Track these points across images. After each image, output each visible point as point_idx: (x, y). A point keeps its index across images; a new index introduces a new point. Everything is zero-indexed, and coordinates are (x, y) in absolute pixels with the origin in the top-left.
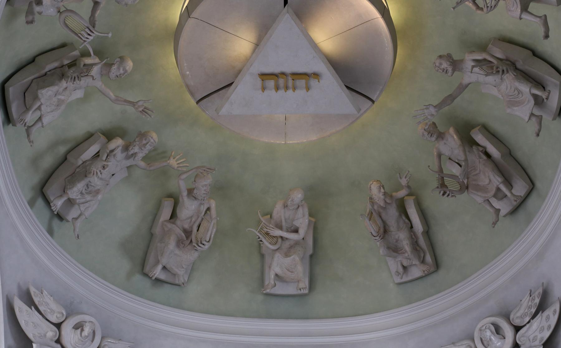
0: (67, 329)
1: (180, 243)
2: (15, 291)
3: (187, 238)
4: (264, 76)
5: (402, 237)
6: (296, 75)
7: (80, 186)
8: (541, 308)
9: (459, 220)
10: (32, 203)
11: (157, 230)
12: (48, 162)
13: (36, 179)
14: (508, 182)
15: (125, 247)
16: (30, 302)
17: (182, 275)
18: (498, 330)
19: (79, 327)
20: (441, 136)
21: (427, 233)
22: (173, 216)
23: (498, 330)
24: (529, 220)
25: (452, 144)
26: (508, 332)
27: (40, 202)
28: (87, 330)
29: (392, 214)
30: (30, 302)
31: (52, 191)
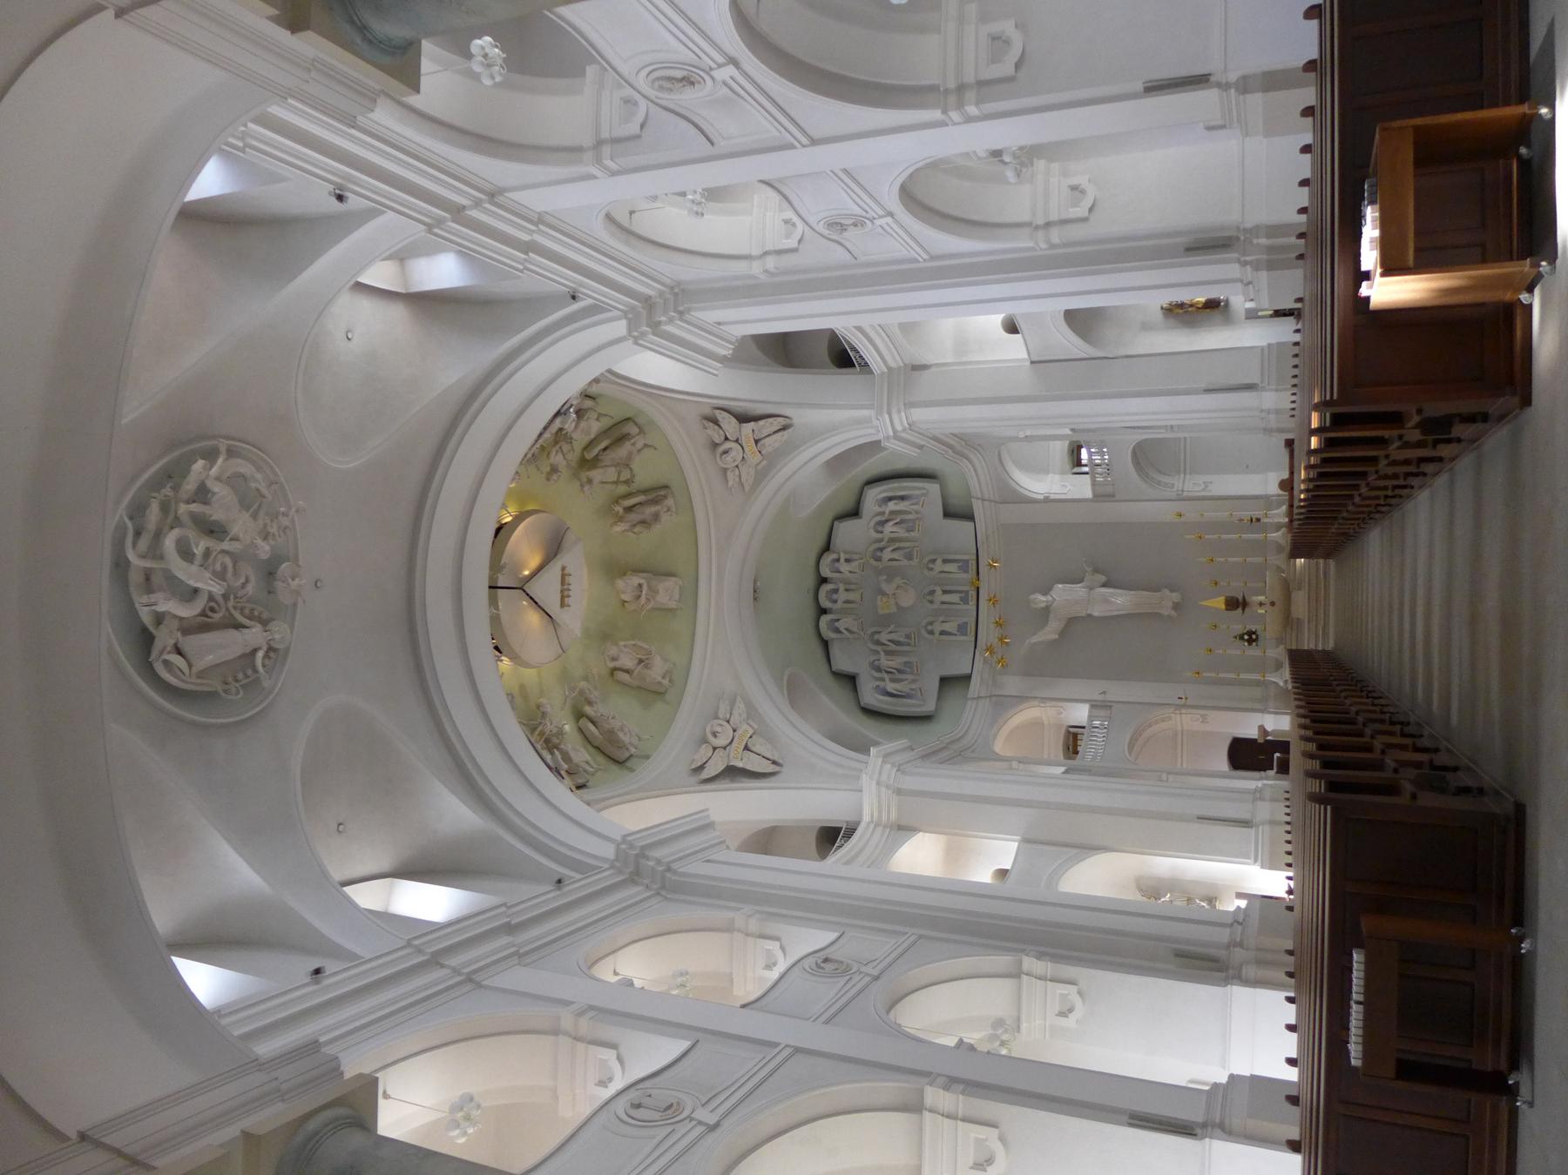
2: (694, 779)
7: (621, 735)
8: (716, 422)
10: (632, 770)
12: (601, 759)
13: (614, 767)
14: (623, 438)
16: (702, 767)
18: (726, 452)
20: (590, 481)
23: (726, 452)
25: (596, 475)
26: (727, 445)
27: (628, 764)
28: (719, 729)
30: (702, 767)
31: (623, 755)
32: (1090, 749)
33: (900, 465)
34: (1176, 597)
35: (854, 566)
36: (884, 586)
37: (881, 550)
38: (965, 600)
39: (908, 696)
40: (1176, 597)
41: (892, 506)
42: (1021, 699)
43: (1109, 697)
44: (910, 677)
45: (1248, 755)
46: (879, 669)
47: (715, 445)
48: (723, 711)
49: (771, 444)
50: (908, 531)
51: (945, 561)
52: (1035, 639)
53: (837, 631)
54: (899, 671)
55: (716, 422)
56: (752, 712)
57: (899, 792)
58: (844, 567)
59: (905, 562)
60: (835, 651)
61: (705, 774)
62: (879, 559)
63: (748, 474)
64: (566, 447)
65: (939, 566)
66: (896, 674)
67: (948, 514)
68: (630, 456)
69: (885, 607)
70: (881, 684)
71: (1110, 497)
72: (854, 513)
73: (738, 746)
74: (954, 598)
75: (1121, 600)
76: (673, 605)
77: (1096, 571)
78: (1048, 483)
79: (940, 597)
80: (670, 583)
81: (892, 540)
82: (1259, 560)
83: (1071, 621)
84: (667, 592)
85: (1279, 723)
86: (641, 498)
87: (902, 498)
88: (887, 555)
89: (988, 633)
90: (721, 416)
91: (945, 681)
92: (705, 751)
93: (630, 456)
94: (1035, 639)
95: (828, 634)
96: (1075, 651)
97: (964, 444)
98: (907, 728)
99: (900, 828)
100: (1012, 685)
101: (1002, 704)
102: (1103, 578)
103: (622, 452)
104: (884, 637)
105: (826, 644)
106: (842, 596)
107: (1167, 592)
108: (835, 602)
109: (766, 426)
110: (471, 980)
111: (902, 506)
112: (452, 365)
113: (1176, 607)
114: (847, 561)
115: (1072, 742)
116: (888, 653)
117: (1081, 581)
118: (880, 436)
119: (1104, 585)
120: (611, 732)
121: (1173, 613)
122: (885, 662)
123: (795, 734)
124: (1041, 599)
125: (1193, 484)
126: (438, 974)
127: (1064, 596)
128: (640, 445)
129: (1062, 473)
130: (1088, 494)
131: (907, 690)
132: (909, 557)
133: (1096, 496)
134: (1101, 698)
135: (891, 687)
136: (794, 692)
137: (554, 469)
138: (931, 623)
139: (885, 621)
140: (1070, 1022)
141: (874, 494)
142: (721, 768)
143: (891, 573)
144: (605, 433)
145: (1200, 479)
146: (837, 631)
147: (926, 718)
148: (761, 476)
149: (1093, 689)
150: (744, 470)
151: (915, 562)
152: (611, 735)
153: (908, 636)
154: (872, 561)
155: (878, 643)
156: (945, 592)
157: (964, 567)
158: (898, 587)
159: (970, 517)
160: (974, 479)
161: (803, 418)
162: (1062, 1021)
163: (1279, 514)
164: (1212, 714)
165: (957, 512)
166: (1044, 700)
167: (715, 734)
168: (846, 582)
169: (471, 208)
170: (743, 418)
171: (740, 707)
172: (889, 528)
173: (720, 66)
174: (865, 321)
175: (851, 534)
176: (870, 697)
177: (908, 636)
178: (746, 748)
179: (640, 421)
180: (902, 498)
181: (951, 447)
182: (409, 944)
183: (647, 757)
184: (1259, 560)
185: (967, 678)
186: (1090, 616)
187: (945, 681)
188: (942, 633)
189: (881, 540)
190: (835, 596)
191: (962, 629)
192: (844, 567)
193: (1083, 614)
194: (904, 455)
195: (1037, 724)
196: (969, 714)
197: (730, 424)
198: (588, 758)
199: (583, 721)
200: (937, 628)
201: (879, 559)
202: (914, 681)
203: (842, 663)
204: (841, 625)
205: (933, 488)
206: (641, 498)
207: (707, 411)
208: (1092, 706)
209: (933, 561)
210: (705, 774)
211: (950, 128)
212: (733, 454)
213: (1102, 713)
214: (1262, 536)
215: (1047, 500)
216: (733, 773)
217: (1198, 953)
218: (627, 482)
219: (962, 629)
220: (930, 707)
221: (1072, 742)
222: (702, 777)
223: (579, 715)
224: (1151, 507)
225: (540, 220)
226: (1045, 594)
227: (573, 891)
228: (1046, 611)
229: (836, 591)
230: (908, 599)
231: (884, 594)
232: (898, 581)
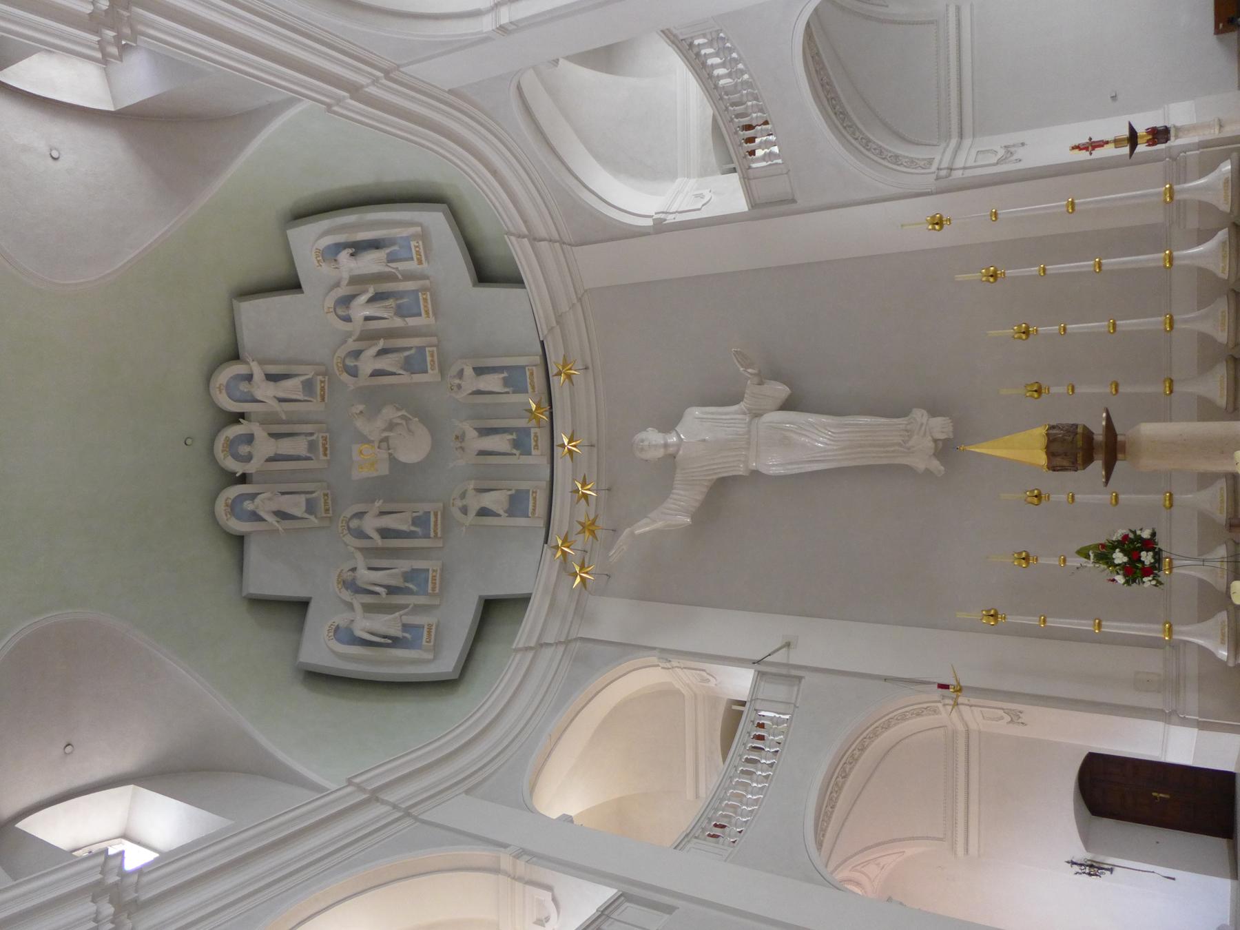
33: (359, 173)
34: (940, 427)
35: (291, 388)
36: (360, 423)
37: (357, 354)
38: (521, 443)
39: (396, 642)
40: (940, 427)
41: (348, 265)
42: (627, 649)
43: (798, 657)
44: (421, 600)
46: (354, 587)
50: (401, 312)
51: (480, 371)
52: (643, 528)
53: (255, 517)
54: (392, 590)
58: (265, 391)
59: (405, 378)
60: (254, 553)
62: (354, 373)
70: (341, 619)
74: (498, 443)
75: (817, 440)
81: (369, 337)
82: (1156, 322)
83: (722, 486)
87: (375, 245)
88: (368, 364)
94: (643, 528)
95: (237, 526)
96: (731, 544)
98: (403, 709)
100: (613, 617)
101: (589, 658)
102: (780, 391)
104: (370, 524)
105: (239, 541)
106: (264, 447)
107: (919, 415)
108: (248, 458)
111: (371, 263)
113: (945, 450)
114: (272, 378)
116: (369, 552)
117: (734, 399)
119: (788, 405)
121: (936, 465)
122: (365, 576)
125: (977, 155)
127: (701, 430)
129: (704, 173)
130: (739, 204)
131: (396, 631)
133: (754, 204)
134: (778, 658)
138: (463, 495)
141: (309, 240)
143: (373, 399)
145: (997, 143)
146: (255, 517)
149: (759, 633)
151: (432, 376)
153: (415, 522)
154: (345, 377)
155: (360, 534)
156: (486, 432)
158: (391, 426)
164: (1032, 712)
165: (487, 272)
166: (667, 654)
168: (268, 420)
172: (360, 309)
176: (320, 648)
177: (421, 521)
180: (375, 245)
181: (354, 90)
184: (1156, 322)
185: (523, 601)
186: (755, 473)
188: (484, 512)
189: (349, 334)
190: (244, 449)
191: (517, 504)
193: (741, 470)
195: (666, 694)
200: (475, 502)
201: (354, 373)
202: (418, 609)
203: (270, 575)
204: (265, 504)
205: (435, 220)
208: (761, 675)
209: (460, 374)
213: (780, 691)
214: (1154, 259)
215: (661, 227)
219: (517, 504)
220: (446, 664)
228: (670, 460)
229: (249, 439)
230: (413, 448)
231: (365, 440)
232: (389, 413)
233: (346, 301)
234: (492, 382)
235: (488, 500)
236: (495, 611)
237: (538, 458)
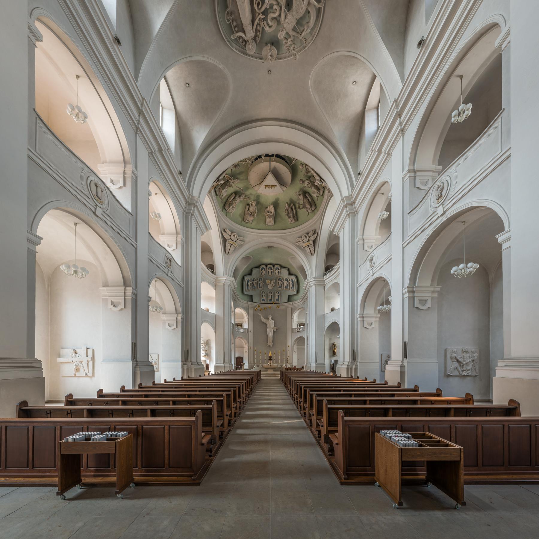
0: (232, 236)
1: (250, 215)
2: (222, 230)
3: (251, 214)
4: (266, 186)
5: (291, 215)
6: (272, 186)
8: (314, 234)
9: (302, 213)
11: (246, 212)
12: (224, 201)
13: (222, 205)
14: (311, 206)
15: (240, 215)
16: (225, 232)
17: (251, 222)
18: (306, 237)
19: (234, 235)
20: (300, 195)
21: (296, 213)
22: (249, 209)
23: (306, 237)
24: (315, 214)
26: (308, 237)
29: (290, 210)
30: (225, 232)
31: (226, 208)
32: (238, 329)
33: (301, 285)
39: (247, 287)
41: (291, 283)
45: (239, 360)
46: (253, 280)
47: (308, 234)
48: (240, 238)
49: (308, 250)
53: (262, 270)
55: (314, 234)
56: (241, 246)
57: (224, 285)
58: (277, 271)
60: (257, 269)
61: (223, 232)
63: (300, 244)
64: (309, 186)
65: (277, 294)
66: (252, 284)
67: (289, 296)
68: (306, 208)
69: (268, 281)
71: (293, 332)
72: (290, 274)
73: (232, 242)
74: (270, 298)
75: (270, 335)
76: (267, 223)
77: (277, 329)
78: (296, 319)
79: (270, 295)
80: (272, 222)
81: (283, 283)
83: (266, 324)
84: (270, 221)
85: (246, 366)
86: (295, 212)
87: (293, 285)
88: (280, 282)
89: (262, 306)
90: (315, 235)
91: (251, 296)
92: (229, 233)
93: (306, 208)
97: (305, 299)
98: (240, 288)
99: (215, 285)
100: (251, 311)
101: (247, 310)
103: (308, 206)
104: (261, 281)
106: (270, 271)
109: (312, 249)
110: (137, 130)
111: (291, 285)
112: (339, 133)
115: (240, 325)
118: (308, 278)
120: (232, 204)
122: (255, 282)
123: (236, 258)
124: (270, 317)
126: (137, 115)
127: (271, 323)
128: (309, 211)
132: (280, 287)
135: (249, 283)
136: (246, 258)
137: (303, 182)
139: (265, 282)
140: (167, 326)
141: (294, 278)
142: (226, 237)
143: (276, 283)
144: (313, 200)
147: (243, 292)
148: (299, 247)
150: (301, 242)
152: (231, 204)
157: (277, 300)
159: (289, 301)
160: (298, 302)
161: (314, 258)
162: (167, 324)
163: (289, 366)
165: (290, 298)
167: (234, 235)
169: (400, 120)
170: (314, 242)
171: (241, 243)
172: (286, 282)
173: (444, 208)
174: (341, 270)
175: (285, 272)
176: (247, 278)
178: (231, 245)
179: (316, 211)
180: (293, 285)
182: (144, 99)
183: (226, 216)
185: (252, 301)
187: (251, 296)
191: (263, 300)
192: (277, 271)
194: (304, 284)
195: (243, 317)
196: (244, 302)
197: (313, 238)
198: (224, 196)
199: (234, 195)
200: (263, 294)
203: (255, 271)
204: (263, 271)
205: (295, 293)
206: (295, 212)
207: (317, 231)
210: (223, 232)
211: (401, 289)
212: (305, 239)
215: (292, 318)
216: (224, 241)
217: (188, 355)
218: (299, 207)
219: (263, 300)
220: (245, 293)
221: (240, 325)
222: (223, 231)
223: (236, 193)
224: (290, 341)
225: (389, 154)
226: (272, 318)
227: (179, 178)
228: (268, 319)
230: (270, 287)
232: (274, 285)
233: (287, 280)
234: (277, 297)
235: (264, 296)
236: (251, 298)
237: (268, 302)
